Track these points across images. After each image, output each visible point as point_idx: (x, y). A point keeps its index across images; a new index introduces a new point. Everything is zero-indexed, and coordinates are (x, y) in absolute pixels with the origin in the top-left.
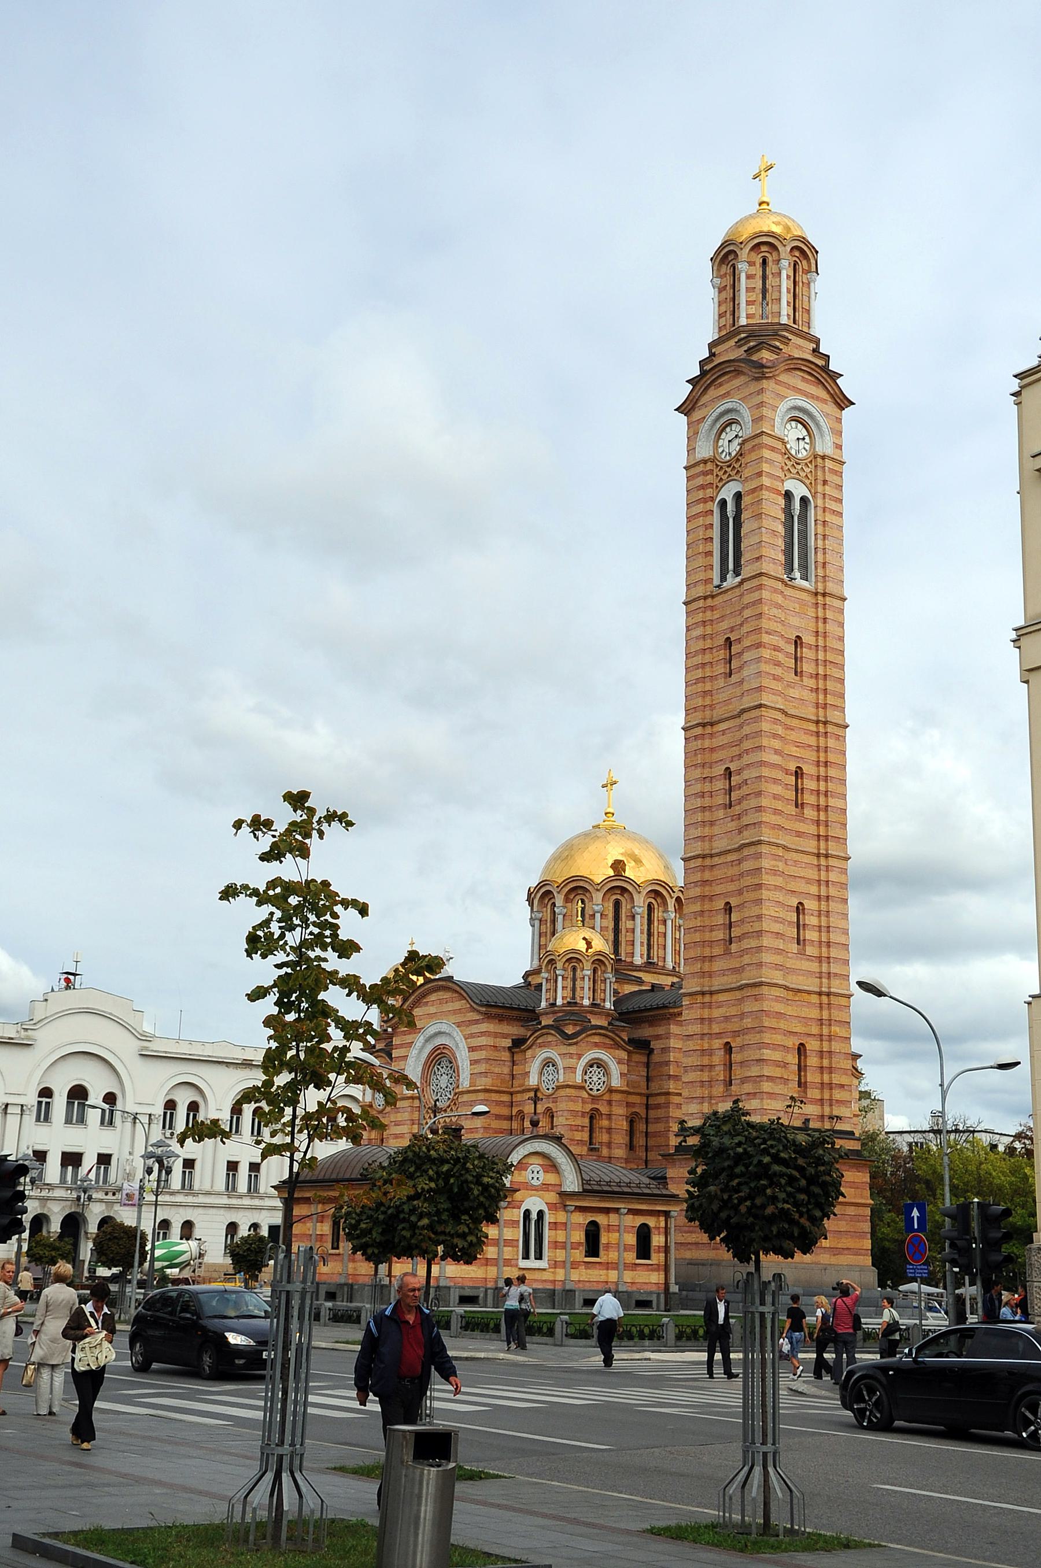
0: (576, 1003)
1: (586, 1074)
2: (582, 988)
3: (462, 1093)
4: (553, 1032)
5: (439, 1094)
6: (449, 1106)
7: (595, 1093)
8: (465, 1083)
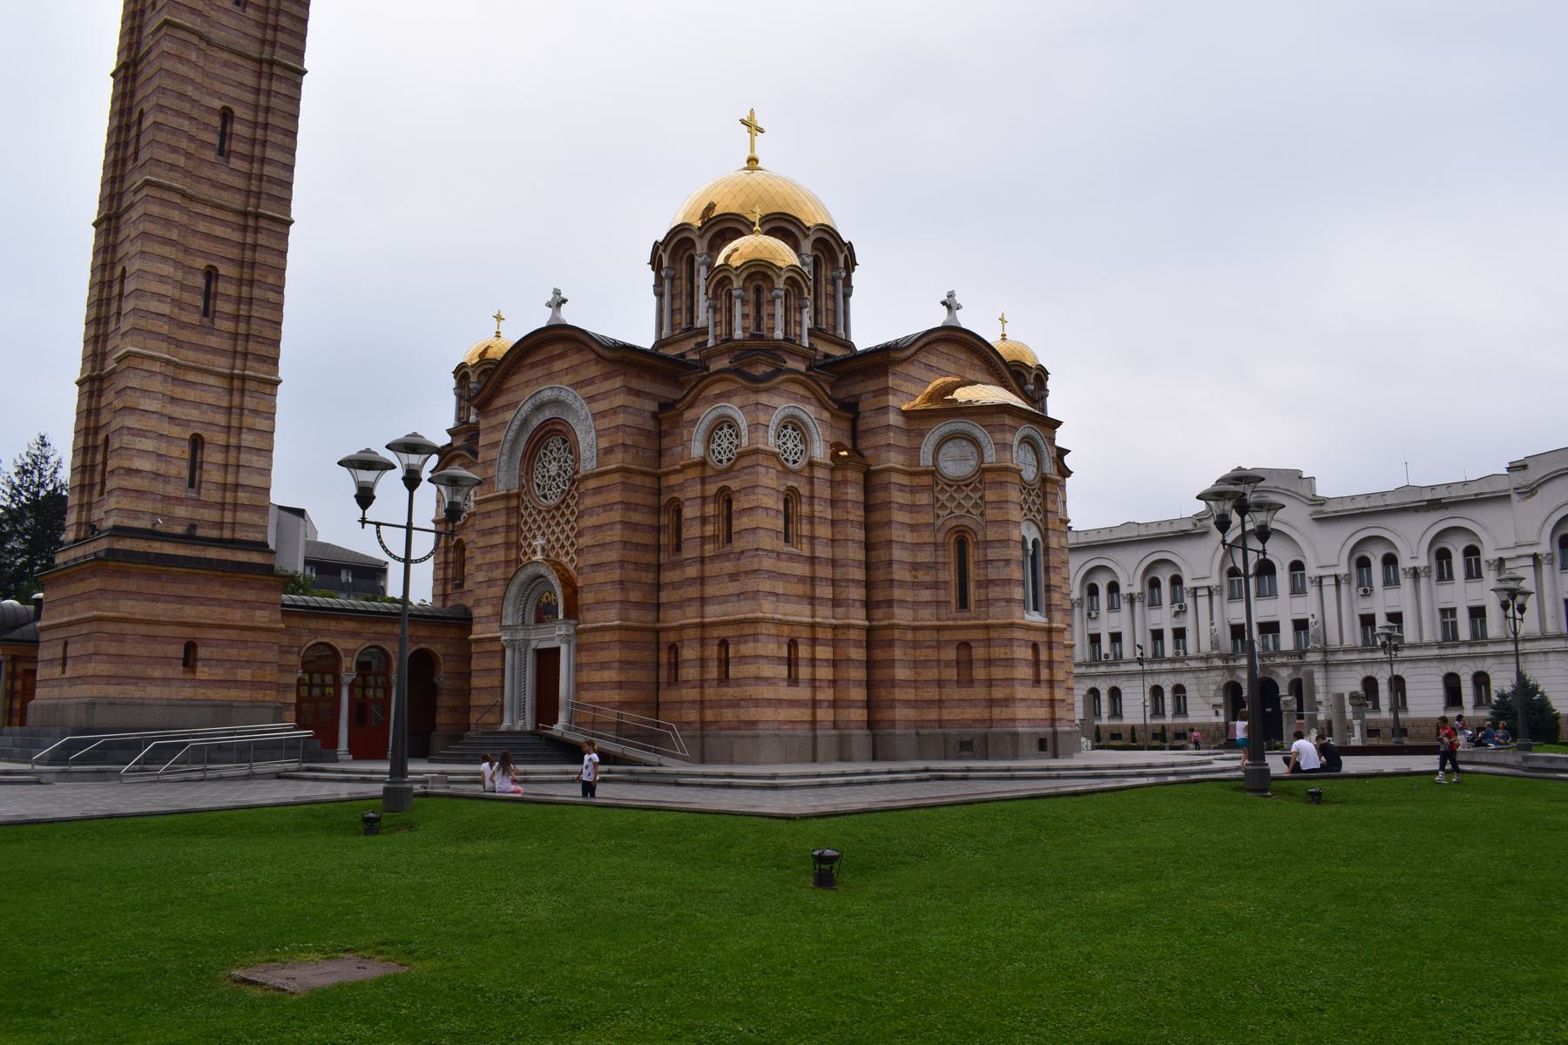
0: (762, 336)
1: (779, 438)
2: (772, 316)
3: (586, 477)
4: (729, 376)
6: (564, 500)
7: (790, 465)
8: (588, 463)
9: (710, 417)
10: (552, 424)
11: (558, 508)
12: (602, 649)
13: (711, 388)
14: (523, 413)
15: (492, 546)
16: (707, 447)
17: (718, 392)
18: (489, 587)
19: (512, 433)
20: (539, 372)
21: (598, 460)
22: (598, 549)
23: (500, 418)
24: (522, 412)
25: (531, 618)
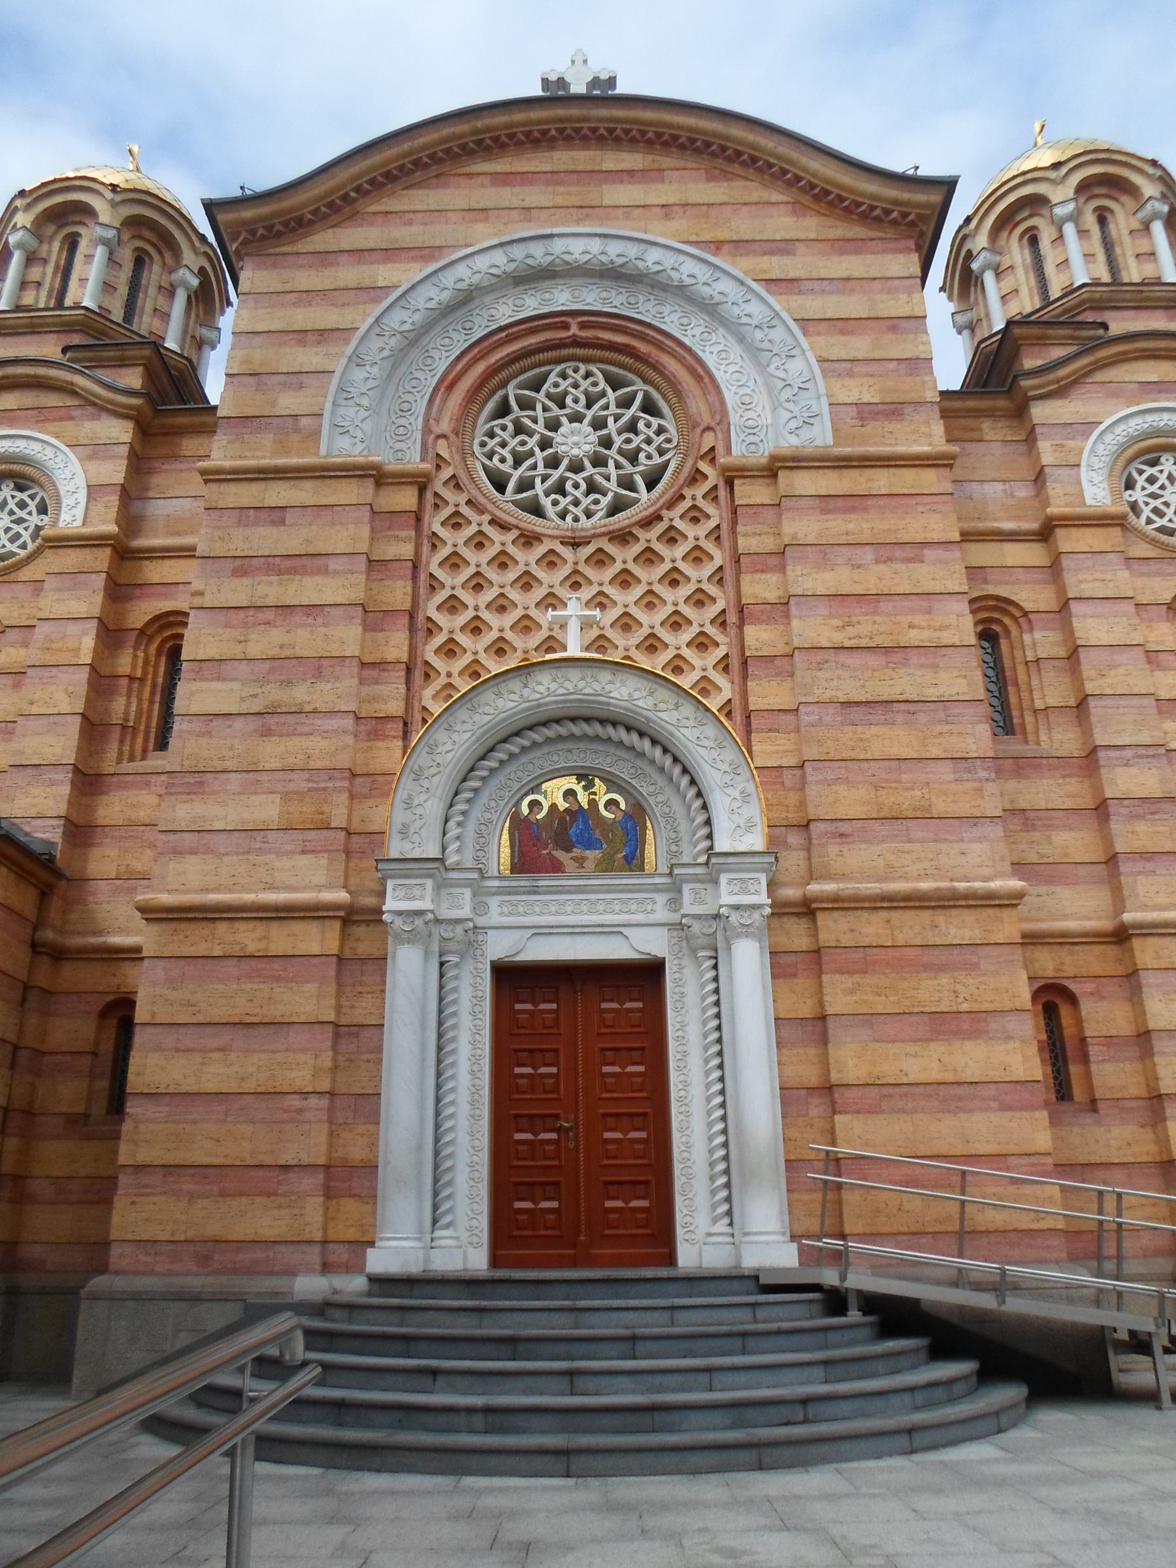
5: (539, 488)
9: (1136, 425)
10: (583, 326)
11: (623, 537)
12: (940, 968)
13: (1126, 367)
14: (464, 275)
15: (286, 609)
16: (1116, 497)
17: (1154, 378)
18: (266, 733)
19: (403, 319)
20: (537, 196)
21: (835, 431)
22: (872, 660)
23: (348, 274)
24: (462, 270)
25: (502, 851)
